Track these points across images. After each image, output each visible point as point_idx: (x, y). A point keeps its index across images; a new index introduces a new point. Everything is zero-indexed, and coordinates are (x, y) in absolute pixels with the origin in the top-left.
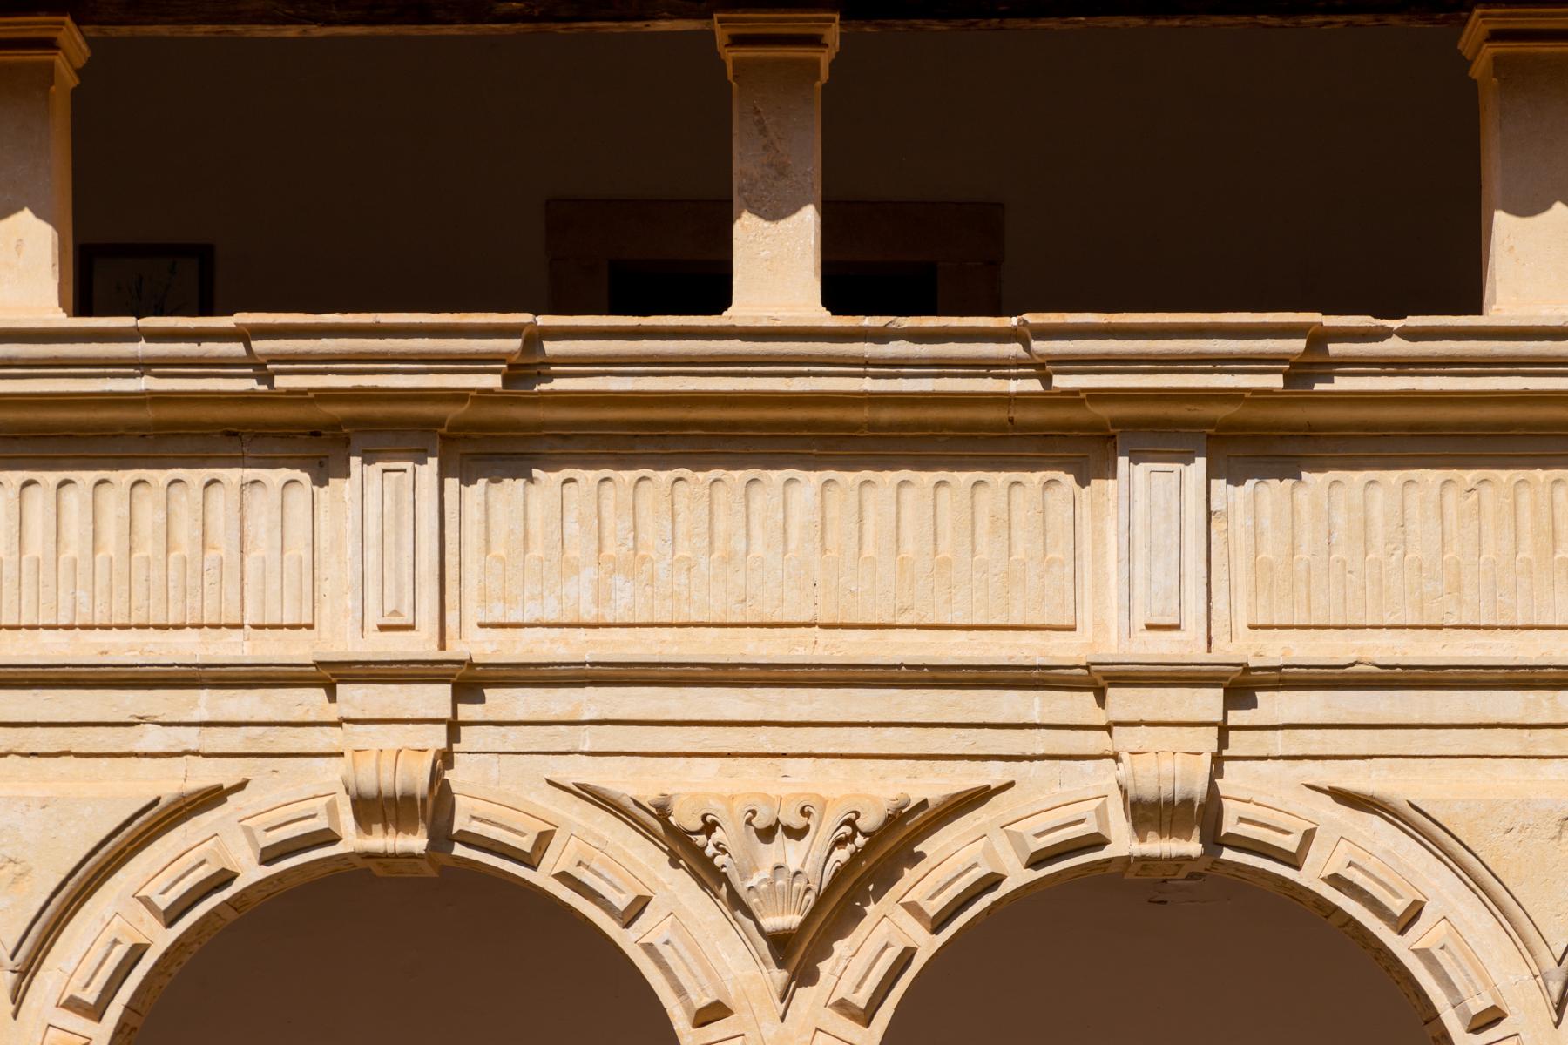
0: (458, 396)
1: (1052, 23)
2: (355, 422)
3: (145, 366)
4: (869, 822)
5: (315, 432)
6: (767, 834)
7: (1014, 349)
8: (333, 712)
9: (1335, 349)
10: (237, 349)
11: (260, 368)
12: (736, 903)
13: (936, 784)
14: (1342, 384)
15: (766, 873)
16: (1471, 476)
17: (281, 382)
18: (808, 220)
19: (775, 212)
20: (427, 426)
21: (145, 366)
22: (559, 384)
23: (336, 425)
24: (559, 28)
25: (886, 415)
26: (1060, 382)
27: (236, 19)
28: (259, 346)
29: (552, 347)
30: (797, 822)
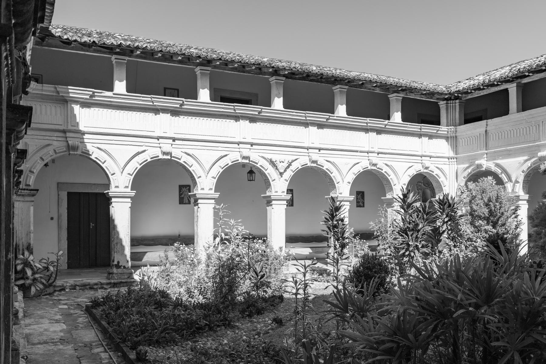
0: (252, 114)
1: (300, 81)
2: (240, 116)
3: (223, 108)
4: (290, 161)
5: (236, 117)
6: (280, 162)
7: (304, 115)
8: (238, 147)
9: (331, 117)
10: (233, 107)
11: (235, 110)
12: (277, 169)
13: (294, 158)
14: (330, 121)
15: (281, 166)
16: (337, 130)
17: (237, 111)
18: (282, 98)
19: (279, 98)
20: (248, 117)
21: (223, 108)
22: (262, 114)
23: (238, 116)
24: (256, 75)
25: (290, 120)
26: (307, 118)
27: (225, 70)
28: (236, 107)
29: (263, 110)
30: (284, 161)
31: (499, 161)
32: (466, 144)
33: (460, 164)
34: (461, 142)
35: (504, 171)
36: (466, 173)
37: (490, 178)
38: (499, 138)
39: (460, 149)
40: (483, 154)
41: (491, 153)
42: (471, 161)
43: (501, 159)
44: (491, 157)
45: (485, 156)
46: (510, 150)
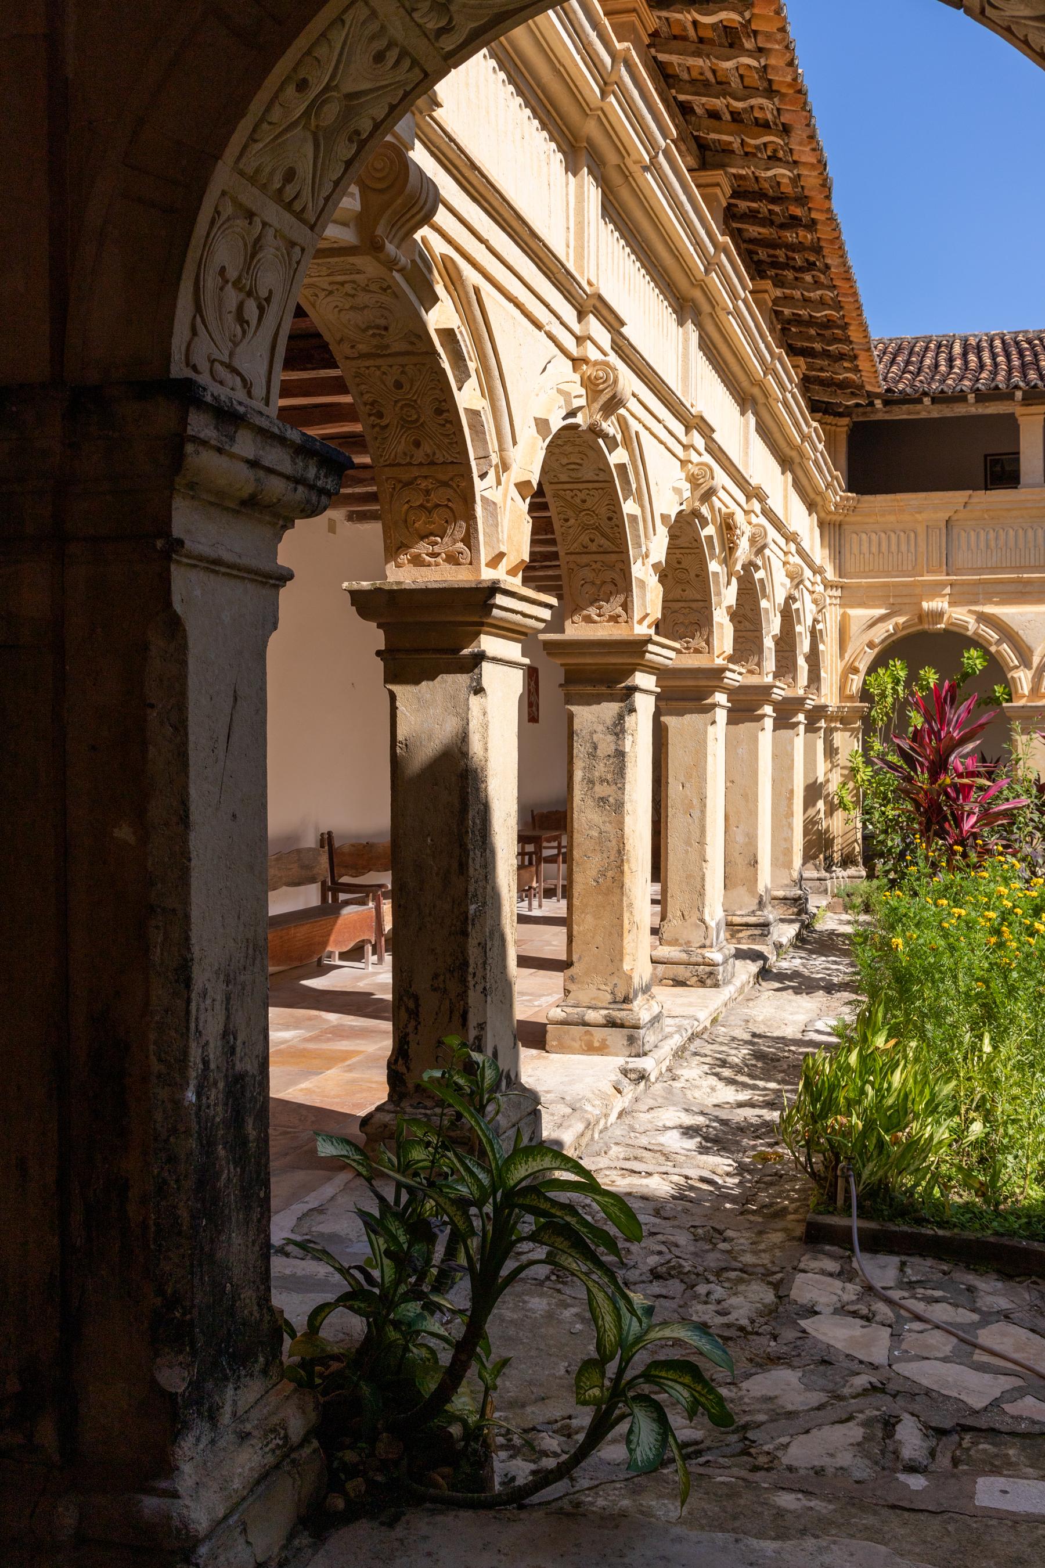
31: (989, 609)
32: (874, 549)
33: (852, 607)
34: (857, 544)
35: (1008, 634)
36: (881, 633)
37: (973, 653)
38: (988, 546)
39: (850, 566)
40: (943, 585)
41: (963, 583)
42: (891, 600)
43: (1003, 602)
44: (962, 596)
45: (948, 590)
46: (1029, 582)
